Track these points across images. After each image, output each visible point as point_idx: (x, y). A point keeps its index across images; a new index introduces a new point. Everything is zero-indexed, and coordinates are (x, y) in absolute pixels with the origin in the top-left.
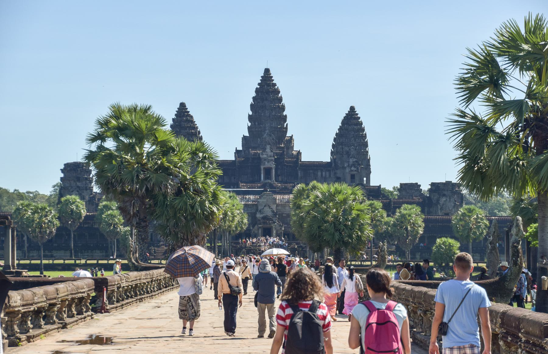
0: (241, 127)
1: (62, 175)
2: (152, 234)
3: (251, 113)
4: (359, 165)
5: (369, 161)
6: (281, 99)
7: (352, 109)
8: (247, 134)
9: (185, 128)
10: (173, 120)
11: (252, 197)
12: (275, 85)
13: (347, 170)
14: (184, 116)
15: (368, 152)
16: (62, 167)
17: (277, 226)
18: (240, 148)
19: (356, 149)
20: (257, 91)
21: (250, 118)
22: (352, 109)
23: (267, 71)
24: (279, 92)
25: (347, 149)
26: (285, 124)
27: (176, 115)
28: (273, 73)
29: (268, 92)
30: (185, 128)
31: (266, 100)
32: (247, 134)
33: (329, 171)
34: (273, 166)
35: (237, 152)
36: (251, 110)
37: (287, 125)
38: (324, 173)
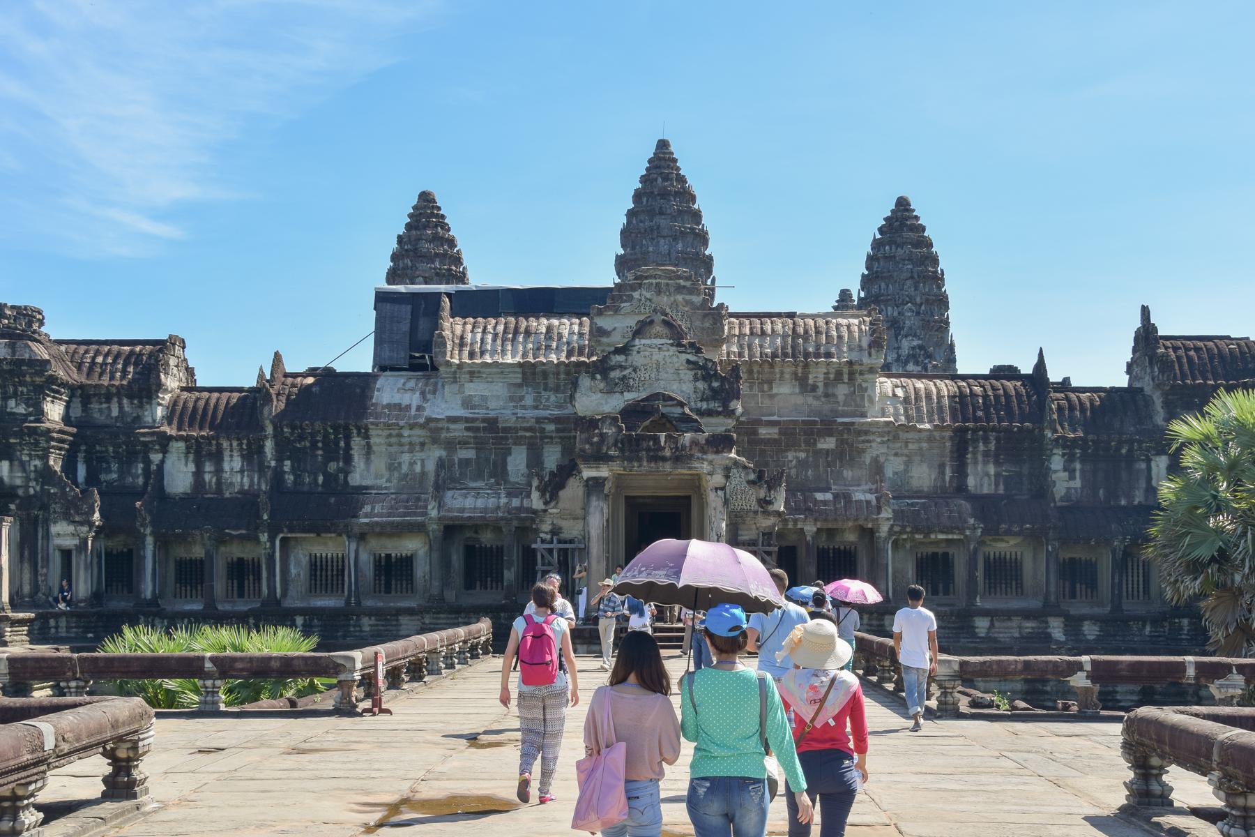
3: (621, 252)
4: (930, 356)
5: (951, 348)
6: (697, 216)
7: (903, 204)
9: (430, 258)
10: (400, 239)
11: (568, 327)
12: (682, 180)
14: (426, 227)
15: (948, 323)
17: (739, 480)
19: (918, 313)
20: (638, 196)
22: (902, 204)
24: (693, 198)
26: (709, 282)
28: (675, 149)
29: (664, 195)
30: (430, 258)
31: (661, 213)
37: (714, 280)
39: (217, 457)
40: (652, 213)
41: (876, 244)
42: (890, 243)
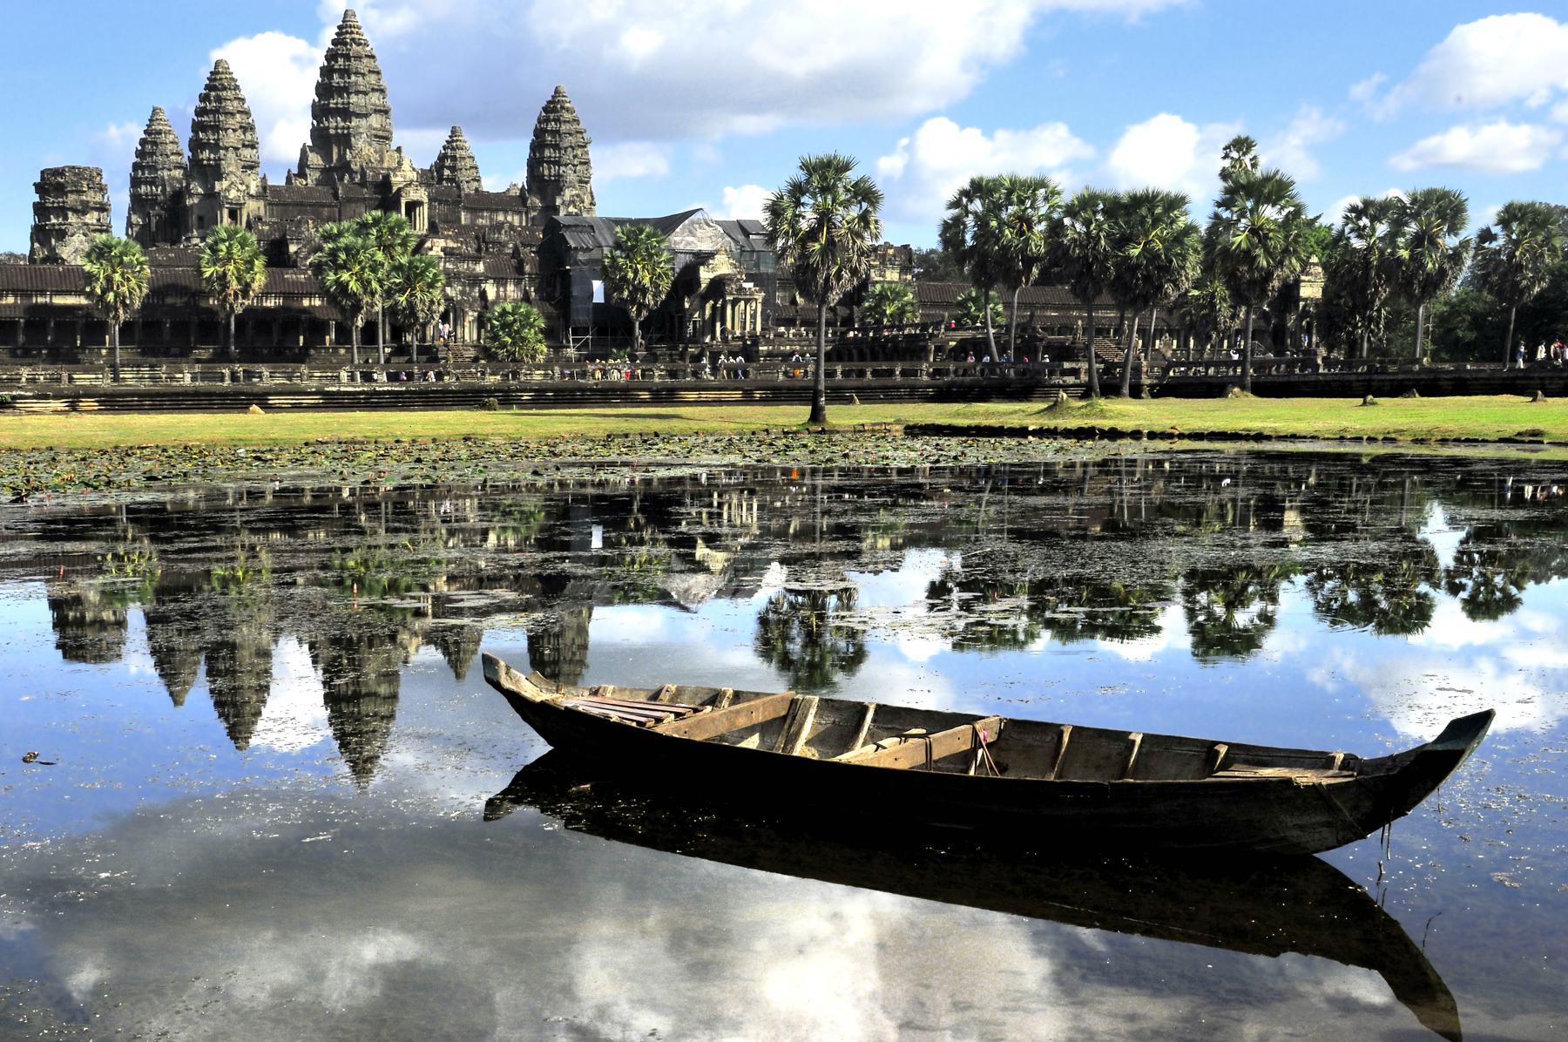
1: (37, 198)
16: (38, 180)
18: (295, 171)
27: (207, 87)
32: (310, 143)
33: (520, 213)
34: (425, 200)
39: (505, 286)
40: (345, 72)
42: (557, 120)
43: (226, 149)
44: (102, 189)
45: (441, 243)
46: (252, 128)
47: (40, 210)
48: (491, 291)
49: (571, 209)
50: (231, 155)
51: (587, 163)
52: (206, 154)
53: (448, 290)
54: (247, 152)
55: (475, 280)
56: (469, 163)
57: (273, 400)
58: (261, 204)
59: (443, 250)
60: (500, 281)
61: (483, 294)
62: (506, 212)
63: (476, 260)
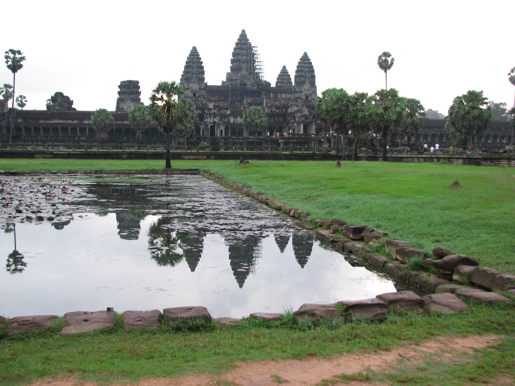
0: (226, 67)
1: (119, 90)
2: (203, 130)
8: (230, 72)
12: (248, 40)
13: (304, 93)
16: (119, 84)
18: (225, 80)
20: (237, 44)
21: (233, 61)
22: (305, 54)
23: (243, 31)
25: (303, 79)
27: (190, 55)
32: (230, 72)
33: (291, 94)
35: (223, 82)
36: (233, 56)
38: (287, 95)
41: (299, 63)
42: (303, 63)
43: (193, 74)
44: (139, 87)
45: (213, 104)
46: (203, 67)
47: (119, 93)
48: (232, 120)
49: (307, 92)
50: (194, 76)
51: (314, 77)
52: (188, 75)
53: (215, 119)
54: (200, 75)
55: (227, 116)
56: (287, 77)
57: (36, 156)
58: (205, 91)
59: (213, 106)
60: (235, 117)
61: (229, 120)
62: (286, 93)
63: (227, 109)
